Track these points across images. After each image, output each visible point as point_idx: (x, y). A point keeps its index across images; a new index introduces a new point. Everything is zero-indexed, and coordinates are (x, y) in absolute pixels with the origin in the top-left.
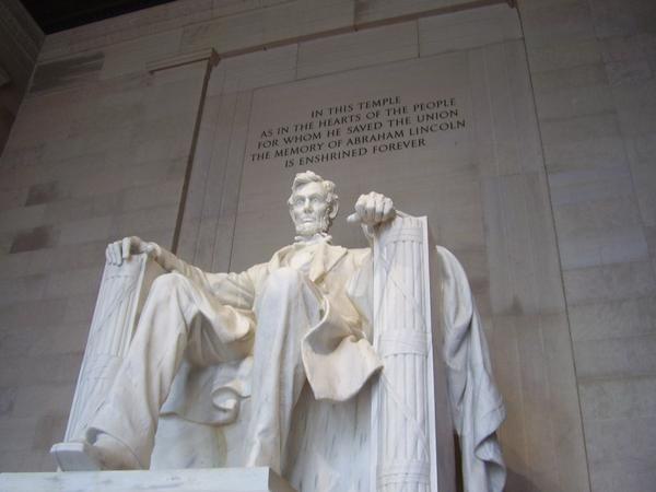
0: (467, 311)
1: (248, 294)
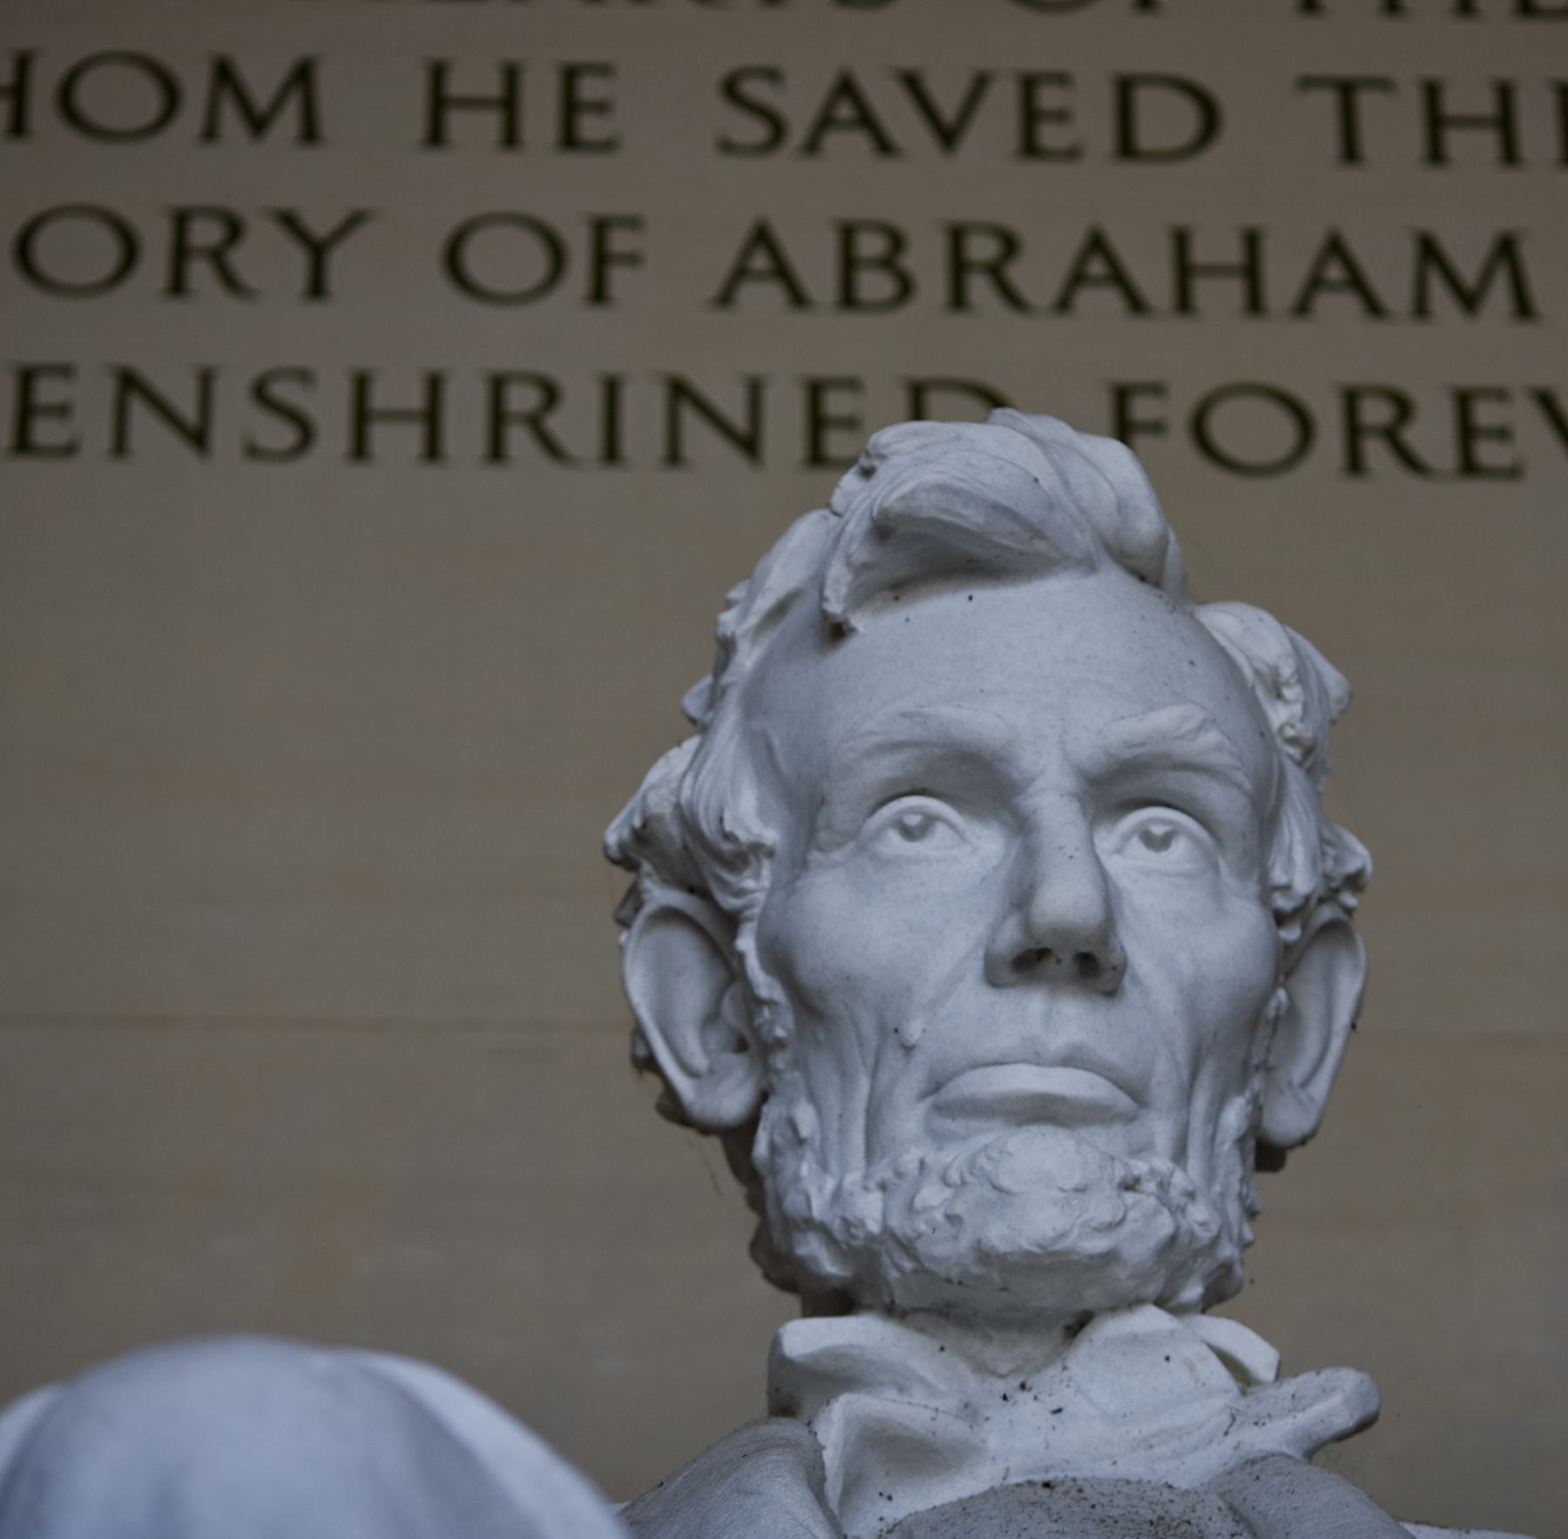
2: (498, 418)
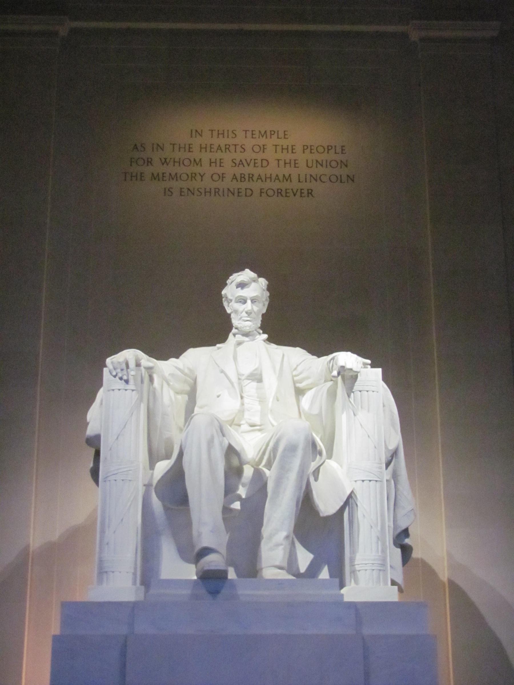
2: (215, 192)
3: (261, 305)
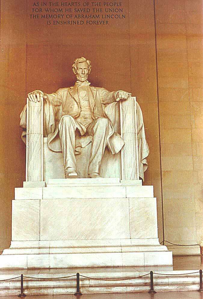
0: (142, 122)
1: (61, 101)
3: (88, 71)
